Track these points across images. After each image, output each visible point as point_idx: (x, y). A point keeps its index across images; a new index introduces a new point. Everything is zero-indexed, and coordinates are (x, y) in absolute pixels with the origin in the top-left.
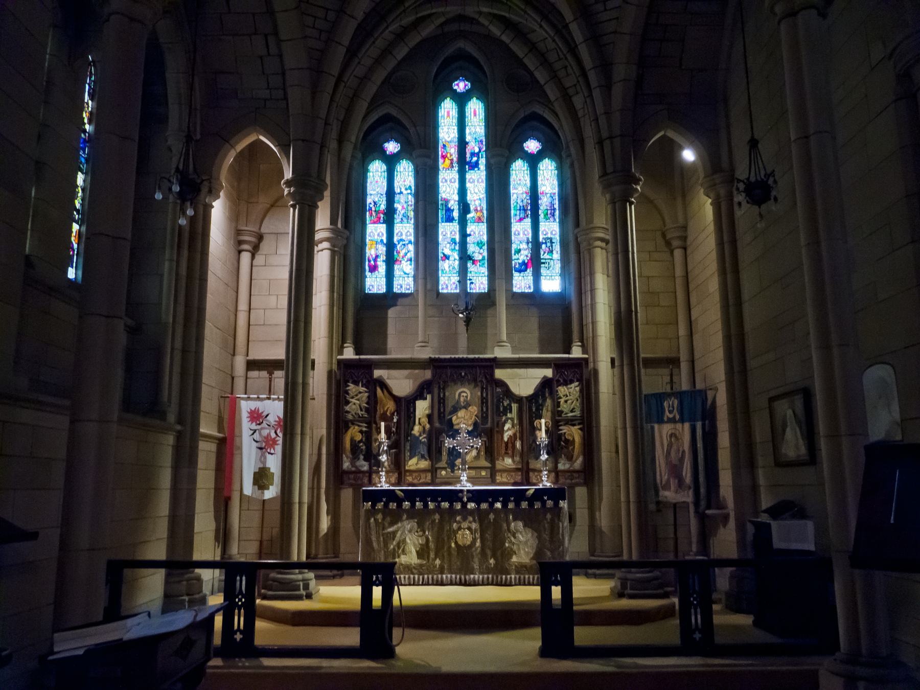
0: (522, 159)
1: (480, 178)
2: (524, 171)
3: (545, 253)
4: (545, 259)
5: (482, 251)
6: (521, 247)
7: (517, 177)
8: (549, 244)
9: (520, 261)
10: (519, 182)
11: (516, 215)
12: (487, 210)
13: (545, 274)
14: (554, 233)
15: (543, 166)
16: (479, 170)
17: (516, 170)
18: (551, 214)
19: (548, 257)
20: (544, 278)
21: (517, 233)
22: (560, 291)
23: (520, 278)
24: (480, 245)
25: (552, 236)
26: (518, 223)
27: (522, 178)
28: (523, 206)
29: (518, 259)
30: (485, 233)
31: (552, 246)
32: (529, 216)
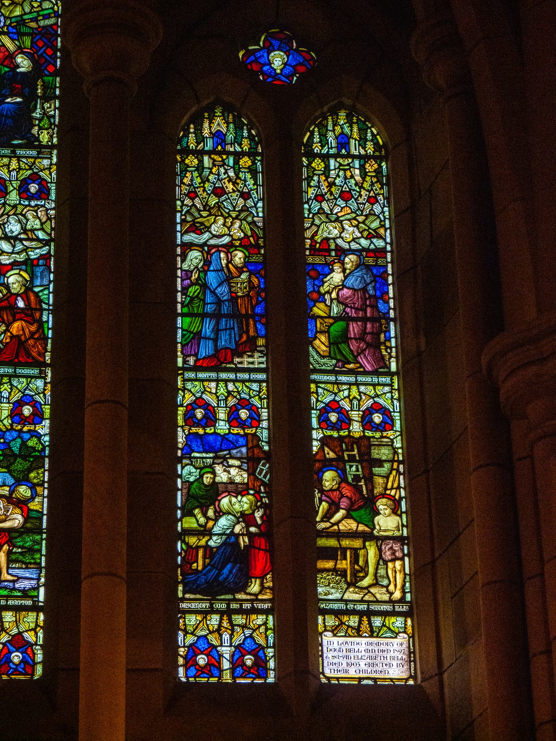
0: (227, 109)
1: (35, 178)
2: (238, 156)
3: (334, 507)
4: (339, 535)
5: (24, 491)
6: (222, 477)
7: (205, 180)
8: (352, 470)
9: (215, 542)
10: (213, 201)
11: (198, 336)
12: (55, 311)
13: (342, 606)
14: (377, 418)
15: (324, 142)
16: (29, 145)
17: (199, 154)
18: (361, 338)
19: (350, 525)
20: (331, 621)
21: (199, 413)
22: (411, 682)
23: (214, 619)
24: (19, 465)
25: (369, 434)
26: (213, 375)
27: (230, 187)
28: (234, 299)
29: (205, 532)
30: (47, 410)
31: (369, 479)
32: (261, 342)
